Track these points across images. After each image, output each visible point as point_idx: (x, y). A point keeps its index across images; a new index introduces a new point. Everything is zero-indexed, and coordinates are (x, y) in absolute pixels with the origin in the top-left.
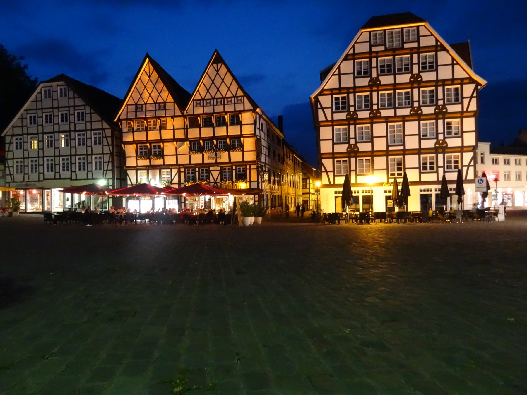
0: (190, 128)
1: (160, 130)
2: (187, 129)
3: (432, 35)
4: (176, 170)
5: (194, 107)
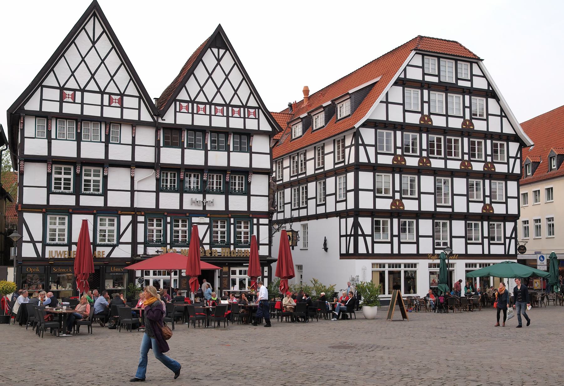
1: (107, 143)
3: (484, 76)
4: (129, 218)
5: (176, 112)
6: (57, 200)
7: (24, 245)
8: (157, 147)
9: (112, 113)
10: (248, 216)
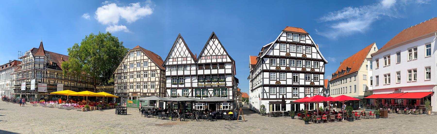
6: (174, 86)
8: (197, 70)
9: (184, 62)
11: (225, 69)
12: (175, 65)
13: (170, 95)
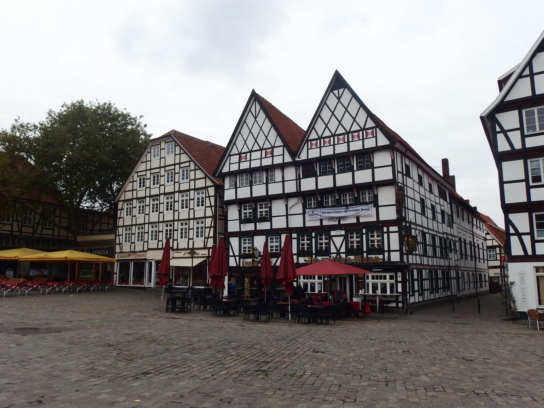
0: (303, 178)
1: (267, 184)
2: (300, 179)
5: (308, 149)
7: (230, 258)
9: (267, 162)
10: (379, 226)
11: (373, 168)
12: (245, 171)
13: (237, 253)
